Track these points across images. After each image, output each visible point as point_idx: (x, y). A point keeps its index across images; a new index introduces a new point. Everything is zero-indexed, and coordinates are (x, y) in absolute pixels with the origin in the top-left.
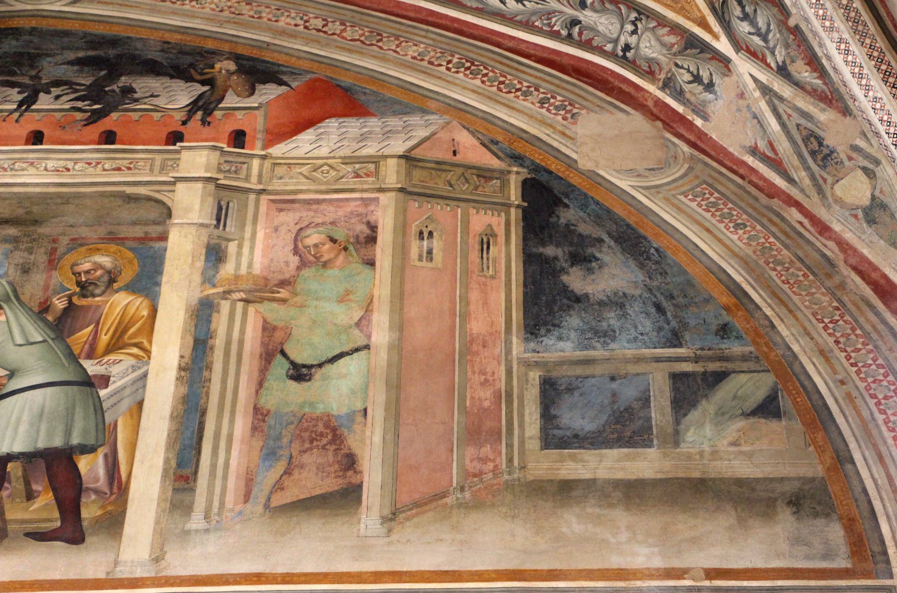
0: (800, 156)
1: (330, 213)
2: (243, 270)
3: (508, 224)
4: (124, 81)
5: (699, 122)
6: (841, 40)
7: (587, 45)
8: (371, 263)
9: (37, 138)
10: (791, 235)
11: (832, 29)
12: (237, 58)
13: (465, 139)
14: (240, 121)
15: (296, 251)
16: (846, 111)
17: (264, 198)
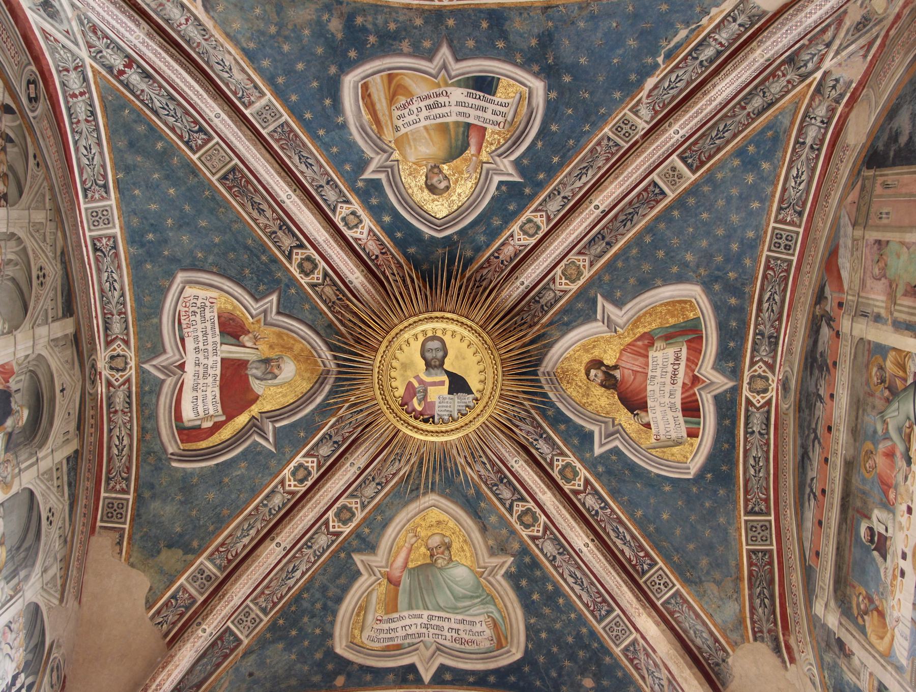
0: (866, 33)
1: (869, 262)
2: (883, 305)
3: (881, 175)
4: (818, 356)
5: (854, 85)
6: (806, 17)
7: (822, 141)
8: (888, 242)
9: (832, 396)
10: (899, 34)
11: (801, 22)
12: (816, 304)
13: (850, 199)
14: (835, 304)
15: (880, 279)
16: (845, 12)
17: (862, 294)
